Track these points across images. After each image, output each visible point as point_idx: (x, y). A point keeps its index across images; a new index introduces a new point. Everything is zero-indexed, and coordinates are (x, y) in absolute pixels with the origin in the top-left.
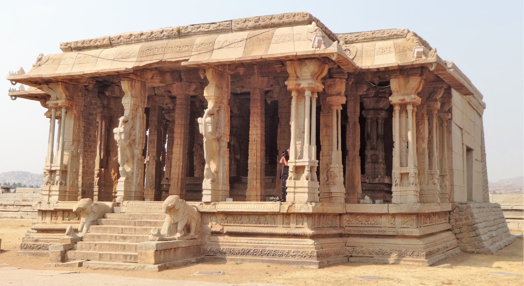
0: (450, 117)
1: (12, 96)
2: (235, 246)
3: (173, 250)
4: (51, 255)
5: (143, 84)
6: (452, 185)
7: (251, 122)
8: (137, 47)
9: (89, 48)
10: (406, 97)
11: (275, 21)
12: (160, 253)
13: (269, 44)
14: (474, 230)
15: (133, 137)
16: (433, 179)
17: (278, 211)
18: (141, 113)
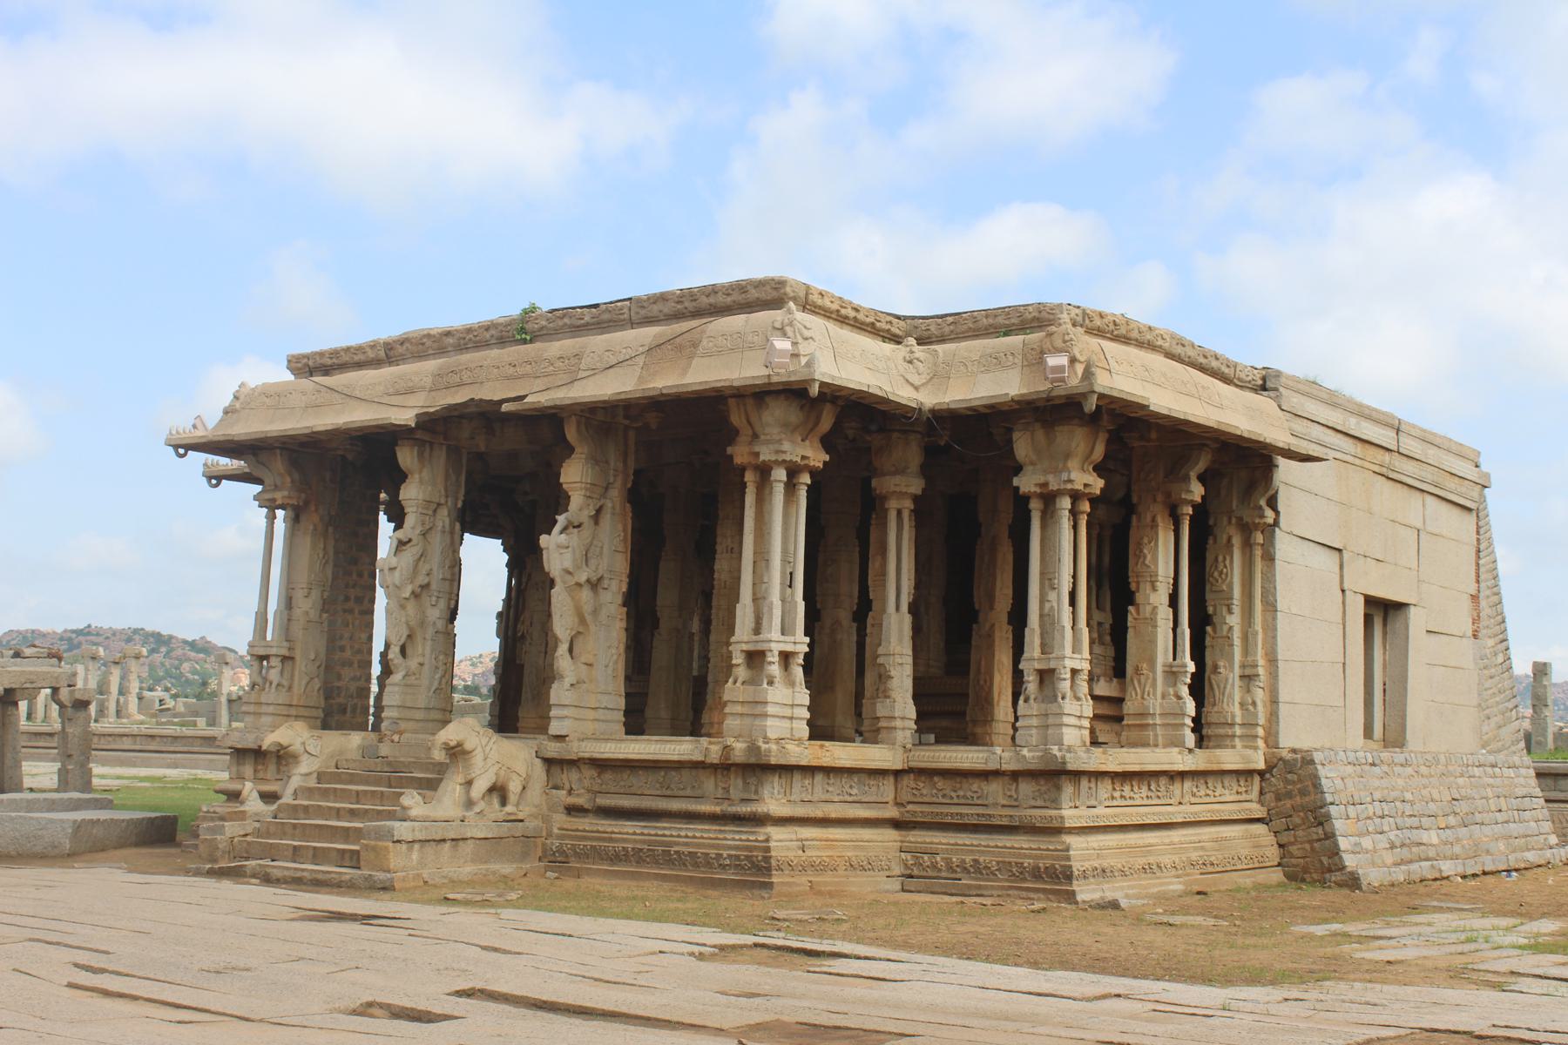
0: (1271, 521)
1: (210, 478)
2: (611, 840)
3: (448, 844)
4: (201, 847)
5: (454, 452)
6: (1274, 701)
7: (719, 540)
8: (431, 365)
9: (343, 367)
10: (1050, 478)
11: (720, 299)
12: (410, 850)
13: (691, 357)
14: (1321, 824)
15: (422, 580)
16: (1175, 685)
17: (701, 758)
18: (447, 521)
